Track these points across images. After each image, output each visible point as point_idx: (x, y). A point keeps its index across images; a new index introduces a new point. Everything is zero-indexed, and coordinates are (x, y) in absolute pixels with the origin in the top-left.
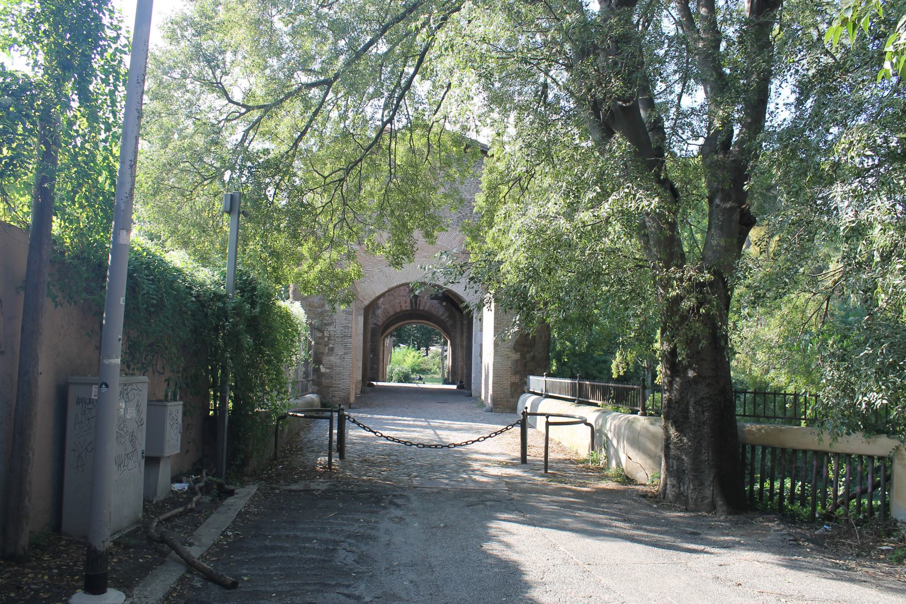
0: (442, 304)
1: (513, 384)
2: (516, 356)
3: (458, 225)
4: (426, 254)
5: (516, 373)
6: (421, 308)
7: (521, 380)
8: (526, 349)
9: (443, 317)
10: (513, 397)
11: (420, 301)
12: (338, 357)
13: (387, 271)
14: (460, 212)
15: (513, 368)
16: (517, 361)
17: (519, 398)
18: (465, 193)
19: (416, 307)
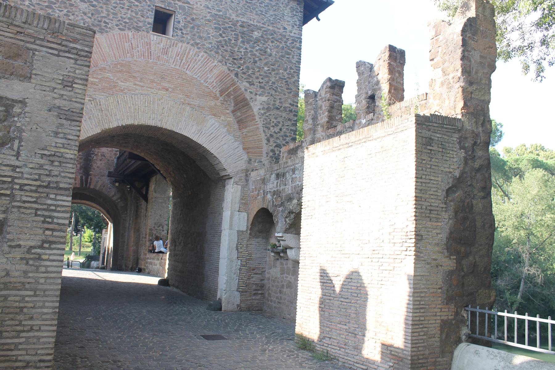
0: (114, 185)
1: (444, 324)
2: (449, 264)
3: (217, 53)
4: (167, 85)
5: (449, 299)
6: (92, 187)
7: (457, 314)
8: (463, 249)
9: (114, 198)
10: (443, 353)
11: (91, 179)
12: (17, 254)
13: (103, 102)
14: (221, 35)
15: (445, 288)
16: (451, 273)
17: (452, 353)
18: (231, 11)
19: (86, 185)
